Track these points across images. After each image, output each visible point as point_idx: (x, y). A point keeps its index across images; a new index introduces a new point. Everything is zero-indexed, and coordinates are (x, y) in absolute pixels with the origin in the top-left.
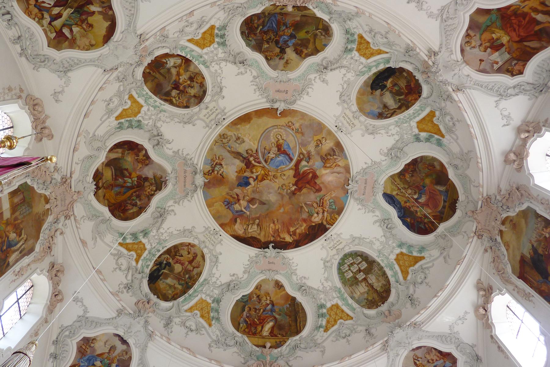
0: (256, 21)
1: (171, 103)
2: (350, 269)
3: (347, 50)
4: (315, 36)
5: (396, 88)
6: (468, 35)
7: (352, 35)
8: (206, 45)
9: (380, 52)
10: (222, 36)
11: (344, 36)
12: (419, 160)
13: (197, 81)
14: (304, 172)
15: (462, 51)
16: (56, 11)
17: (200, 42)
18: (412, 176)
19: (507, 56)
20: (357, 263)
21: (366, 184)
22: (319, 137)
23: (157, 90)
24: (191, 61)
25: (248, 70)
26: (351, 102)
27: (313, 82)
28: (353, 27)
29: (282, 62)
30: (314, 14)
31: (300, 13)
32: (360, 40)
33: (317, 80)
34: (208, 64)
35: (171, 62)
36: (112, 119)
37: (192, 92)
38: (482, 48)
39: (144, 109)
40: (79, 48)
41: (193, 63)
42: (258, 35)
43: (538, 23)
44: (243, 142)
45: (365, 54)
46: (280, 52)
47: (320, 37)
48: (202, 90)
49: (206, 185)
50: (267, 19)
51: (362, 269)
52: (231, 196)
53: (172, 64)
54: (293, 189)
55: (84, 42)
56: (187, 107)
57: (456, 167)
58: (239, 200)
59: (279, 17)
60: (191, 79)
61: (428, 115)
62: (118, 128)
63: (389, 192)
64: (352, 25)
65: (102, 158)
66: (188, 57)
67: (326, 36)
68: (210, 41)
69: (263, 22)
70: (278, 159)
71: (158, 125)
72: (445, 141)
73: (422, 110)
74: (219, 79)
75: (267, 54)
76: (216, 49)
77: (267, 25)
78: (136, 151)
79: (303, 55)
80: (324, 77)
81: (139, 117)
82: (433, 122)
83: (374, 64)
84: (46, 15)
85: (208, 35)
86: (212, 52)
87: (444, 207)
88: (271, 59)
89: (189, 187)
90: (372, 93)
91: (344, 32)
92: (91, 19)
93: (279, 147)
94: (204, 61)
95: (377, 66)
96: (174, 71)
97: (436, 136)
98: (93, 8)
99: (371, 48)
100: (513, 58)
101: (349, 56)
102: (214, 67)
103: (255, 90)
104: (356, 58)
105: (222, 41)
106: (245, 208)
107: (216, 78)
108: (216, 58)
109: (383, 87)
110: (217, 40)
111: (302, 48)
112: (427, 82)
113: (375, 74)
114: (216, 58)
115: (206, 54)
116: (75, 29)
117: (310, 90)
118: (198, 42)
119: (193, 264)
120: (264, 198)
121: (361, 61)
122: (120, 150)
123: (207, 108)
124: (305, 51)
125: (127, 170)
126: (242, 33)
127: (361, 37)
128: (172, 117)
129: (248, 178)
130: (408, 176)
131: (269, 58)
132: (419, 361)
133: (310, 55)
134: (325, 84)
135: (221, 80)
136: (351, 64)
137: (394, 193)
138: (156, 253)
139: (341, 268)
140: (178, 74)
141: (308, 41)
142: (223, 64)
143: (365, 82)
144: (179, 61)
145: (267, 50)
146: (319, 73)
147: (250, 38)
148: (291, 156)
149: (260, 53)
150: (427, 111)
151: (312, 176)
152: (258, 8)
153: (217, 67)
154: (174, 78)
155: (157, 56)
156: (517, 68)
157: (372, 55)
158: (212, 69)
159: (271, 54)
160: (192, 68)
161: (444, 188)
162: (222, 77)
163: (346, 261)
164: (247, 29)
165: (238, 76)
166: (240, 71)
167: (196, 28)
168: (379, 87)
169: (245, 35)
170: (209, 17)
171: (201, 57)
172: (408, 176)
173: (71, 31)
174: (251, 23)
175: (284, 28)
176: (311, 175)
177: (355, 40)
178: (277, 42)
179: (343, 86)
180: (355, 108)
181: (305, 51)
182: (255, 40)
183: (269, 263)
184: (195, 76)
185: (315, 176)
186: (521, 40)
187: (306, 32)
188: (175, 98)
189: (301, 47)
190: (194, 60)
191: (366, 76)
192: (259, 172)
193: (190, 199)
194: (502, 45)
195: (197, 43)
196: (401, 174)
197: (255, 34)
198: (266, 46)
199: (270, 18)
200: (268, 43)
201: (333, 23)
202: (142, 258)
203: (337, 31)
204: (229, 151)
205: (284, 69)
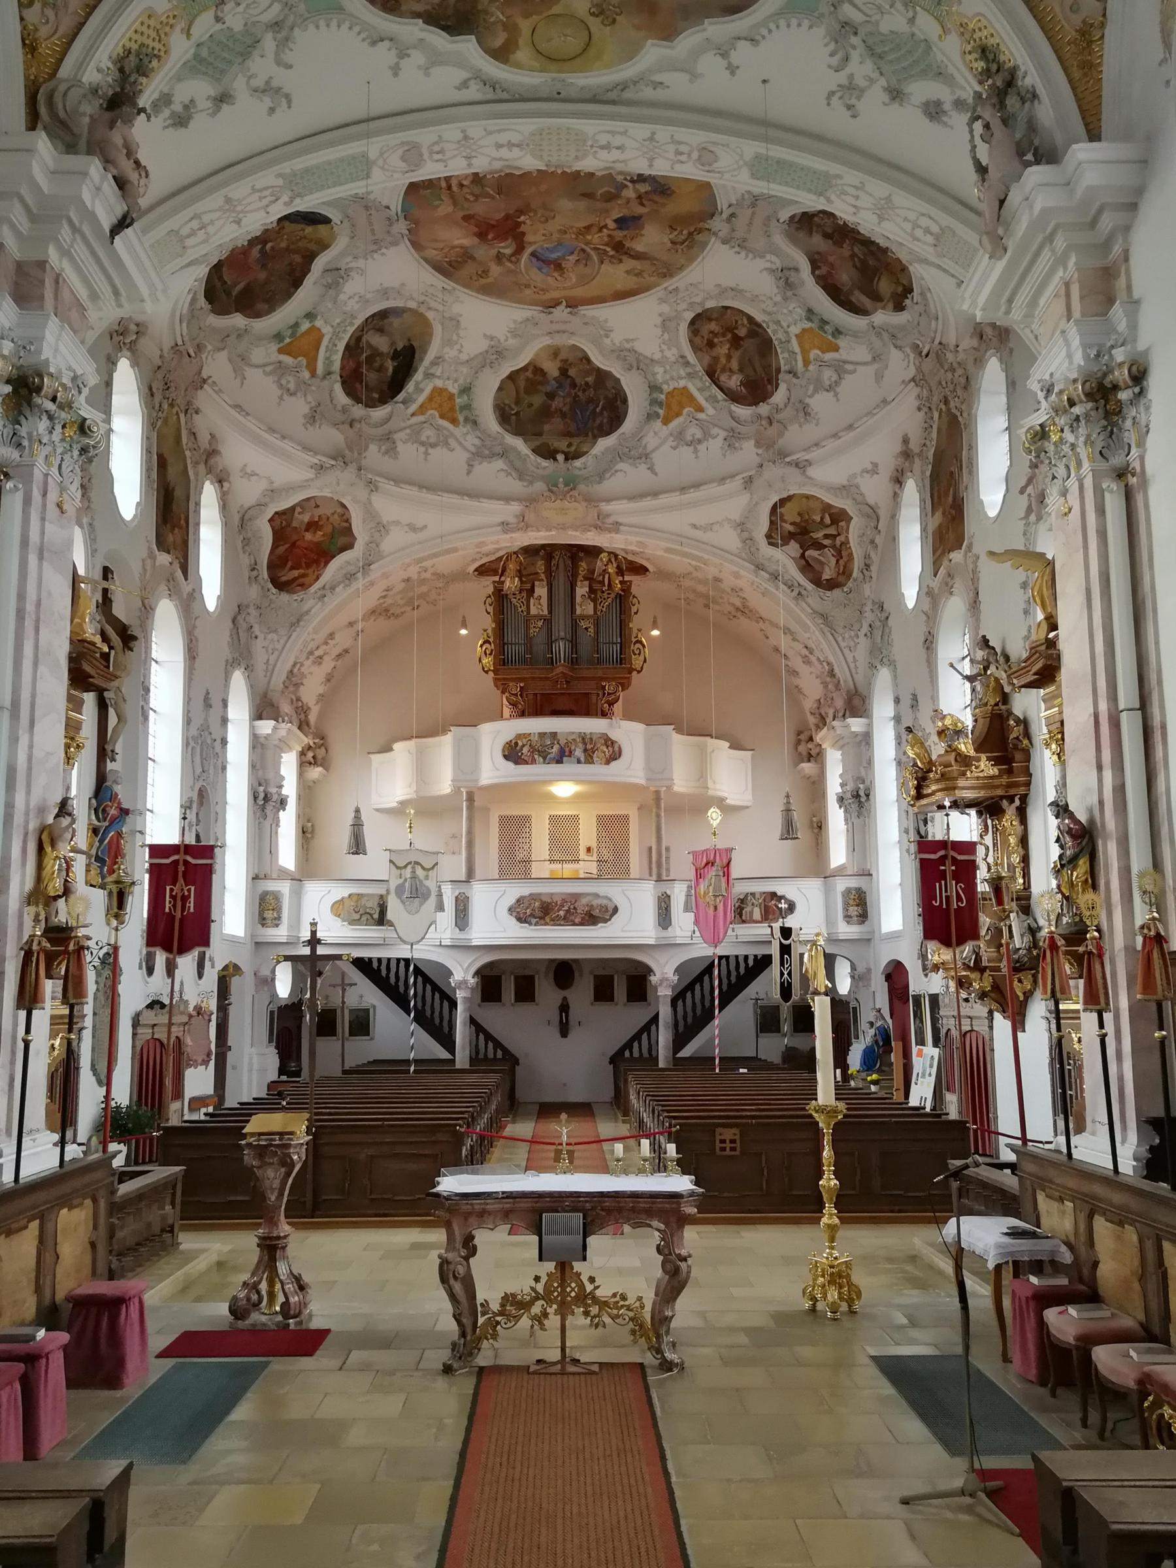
1: (750, 319)
3: (466, 390)
4: (517, 403)
5: (376, 365)
6: (348, 521)
9: (422, 409)
10: (654, 402)
11: (477, 413)
12: (292, 290)
14: (507, 239)
15: (344, 506)
16: (827, 542)
18: (290, 264)
19: (294, 524)
21: (373, 230)
22: (483, 281)
23: (766, 346)
29: (563, 355)
35: (734, 382)
36: (843, 354)
37: (713, 326)
38: (324, 517)
39: (795, 330)
40: (822, 501)
42: (602, 397)
43: (292, 568)
44: (627, 272)
49: (713, 215)
52: (656, 202)
53: (734, 377)
54: (522, 218)
55: (812, 504)
56: (726, 308)
57: (241, 334)
58: (640, 197)
60: (711, 345)
61: (315, 359)
62: (840, 333)
63: (321, 227)
64: (471, 441)
65: (882, 317)
70: (559, 254)
71: (778, 298)
72: (274, 347)
73: (327, 359)
74: (666, 336)
76: (666, 382)
78: (830, 281)
81: (808, 325)
82: (304, 356)
83: (421, 386)
84: (838, 542)
86: (672, 379)
87: (220, 278)
89: (744, 215)
91: (479, 420)
92: (798, 520)
93: (558, 266)
95: (417, 383)
96: (735, 364)
97: (288, 340)
98: (791, 528)
100: (289, 525)
101: (461, 381)
102: (671, 354)
106: (626, 186)
109: (395, 355)
110: (663, 397)
112: (344, 410)
113: (416, 370)
116: (818, 518)
120: (582, 204)
122: (854, 299)
123: (692, 304)
124: (529, 374)
125: (854, 266)
126: (625, 401)
127: (454, 421)
128: (754, 299)
129: (620, 228)
130: (298, 259)
137: (309, 230)
140: (729, 357)
143: (425, 352)
144: (723, 378)
145: (588, 373)
148: (534, 260)
150: (320, 368)
151: (487, 235)
152: (603, 449)
153: (668, 354)
154: (736, 355)
155: (750, 405)
156: (278, 522)
157: (430, 398)
158: (674, 351)
159: (581, 367)
160: (707, 359)
161: (234, 293)
171: (689, 374)
172: (298, 259)
173: (822, 519)
176: (490, 237)
178: (573, 385)
180: (430, 315)
181: (529, 374)
185: (482, 236)
186: (294, 545)
188: (743, 325)
191: (426, 362)
192: (596, 238)
193: (746, 196)
194: (307, 530)
195: (691, 399)
196: (310, 257)
197: (606, 398)
198: (590, 379)
200: (587, 383)
204: (656, 259)
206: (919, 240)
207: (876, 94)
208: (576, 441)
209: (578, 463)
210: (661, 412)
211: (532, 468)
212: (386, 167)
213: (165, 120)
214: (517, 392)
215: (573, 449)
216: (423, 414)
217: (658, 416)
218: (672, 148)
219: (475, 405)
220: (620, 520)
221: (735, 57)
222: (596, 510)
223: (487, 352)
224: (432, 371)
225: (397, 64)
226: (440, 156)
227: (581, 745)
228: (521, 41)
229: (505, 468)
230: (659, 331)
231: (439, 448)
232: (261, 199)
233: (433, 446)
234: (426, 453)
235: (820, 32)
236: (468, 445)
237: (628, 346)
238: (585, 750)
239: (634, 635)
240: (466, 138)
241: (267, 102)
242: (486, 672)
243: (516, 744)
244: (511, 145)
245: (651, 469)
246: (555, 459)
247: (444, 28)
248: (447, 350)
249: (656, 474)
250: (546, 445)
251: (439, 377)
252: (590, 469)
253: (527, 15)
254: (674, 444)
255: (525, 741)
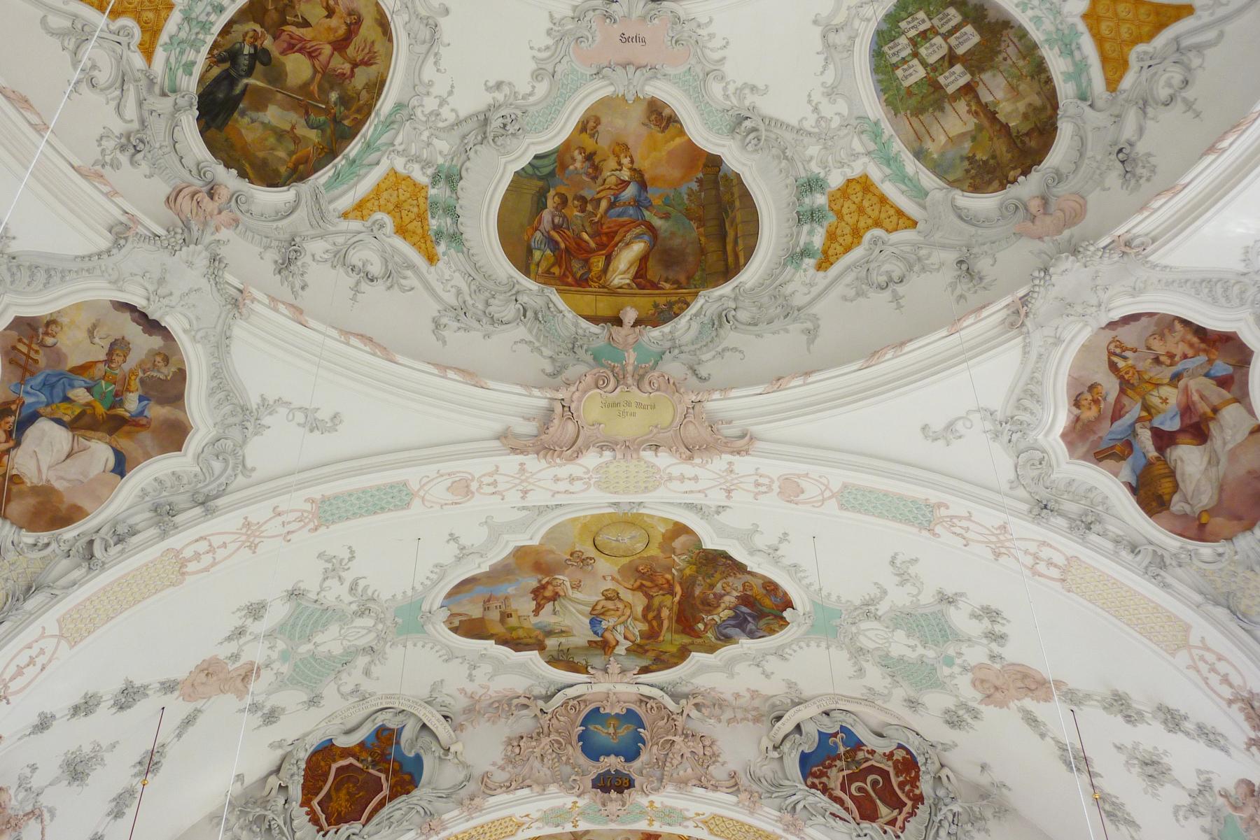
2: (915, 55)
20: (944, 30)
51: (960, 51)
119: (351, 51)
132: (1125, 358)
138: (213, 18)
139: (886, 49)
163: (903, 25)
183: (625, 39)
202: (164, 38)
206: (197, 541)
207: (311, 585)
212: (823, 488)
213: (1003, 625)
218: (500, 487)
221: (453, 549)
225: (780, 542)
226: (761, 481)
228: (660, 539)
232: (967, 529)
235: (385, 595)
240: (729, 491)
241: (913, 570)
244: (682, 478)
247: (730, 558)
253: (652, 558)
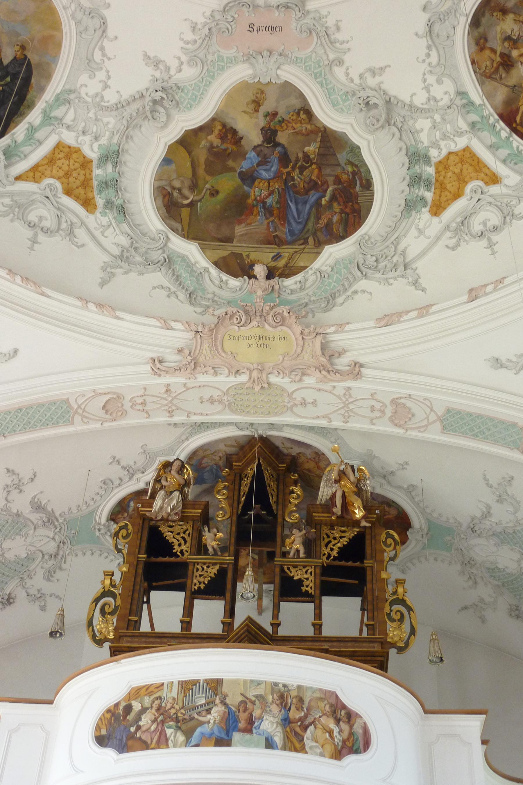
0: (335, 219)
4: (194, 186)
7: (109, 204)
8: (457, 159)
11: (127, 195)
13: (492, 56)
17: (471, 169)
24: (501, 116)
25: (357, 81)
26: (73, 16)
27: (184, 58)
28: (111, 228)
29: (268, 106)
30: (203, 249)
31: (235, 247)
32: (90, 195)
33: (174, 64)
34: (459, 102)
41: (495, 109)
42: (331, 179)
45: (68, 157)
46: (274, 133)
47: (182, 182)
48: (481, 29)
50: (310, 225)
59: (283, 232)
66: (504, 131)
67: (169, 189)
68: (446, 168)
69: (318, 218)
74: (434, 58)
75: (309, 127)
77: (311, 208)
79: (218, 127)
80: (157, 74)
83: (39, 135)
85: (449, 186)
86: (445, 137)
88: (298, 114)
90: (23, 48)
91: (131, 208)
94: (468, 112)
95: (32, 130)
99: (59, 179)
101: (104, 141)
103: (338, 29)
104: (87, 139)
105: (417, 167)
107: (442, 61)
108: (437, 118)
110: (430, 170)
111: (222, 147)
113: (31, 106)
114: (437, 118)
115: (460, 134)
117: (189, 36)
118: (477, 171)
121: (74, 134)
126: (368, 185)
131: (303, 116)
133: (201, 129)
134: (151, 54)
135: (428, 55)
136: (97, 120)
141: (211, 171)
142: (420, 100)
143: (48, 76)
146: (171, 83)
147: (350, 169)
149: (325, 128)
152: (331, 261)
153: (437, 91)
158: (448, 86)
159: (298, 127)
162: (426, 65)
164: (357, 196)
165: (382, 65)
166: (378, 79)
167: (474, 216)
168: (10, 69)
169: (361, 179)
170: (441, 243)
171: (473, 125)
174: (347, 214)
175: (269, 201)
177: (100, 192)
178: (285, 159)
179: (104, 55)
181: (214, 139)
182: (339, 165)
184: (497, 70)
187: (217, 192)
189: (225, 150)
190: (492, 120)
197: (338, 180)
198: (312, 149)
199: (304, 227)
200: (307, 157)
201: (159, 232)
203: (146, 209)
205: (263, 88)
208: (286, 251)
209: (290, 282)
210: (429, 196)
211: (211, 287)
214: (194, 166)
215: (281, 263)
216: (35, 180)
217: (423, 199)
219: (124, 182)
220: (362, 360)
222: (319, 339)
223: (147, 89)
224: (58, 113)
227: (275, 709)
229: (166, 284)
230: (424, 42)
231: (57, 238)
233: (46, 231)
234: (34, 241)
236: (107, 243)
237: (372, 82)
238: (286, 722)
239: (390, 589)
242: (99, 643)
243: (128, 709)
245: (415, 284)
246: (252, 276)
248: (84, 79)
249: (423, 290)
250: (237, 256)
251: (68, 127)
252: (310, 291)
254: (452, 242)
255: (147, 701)
